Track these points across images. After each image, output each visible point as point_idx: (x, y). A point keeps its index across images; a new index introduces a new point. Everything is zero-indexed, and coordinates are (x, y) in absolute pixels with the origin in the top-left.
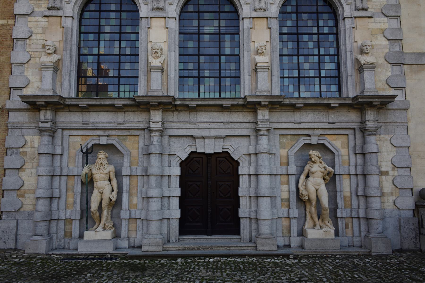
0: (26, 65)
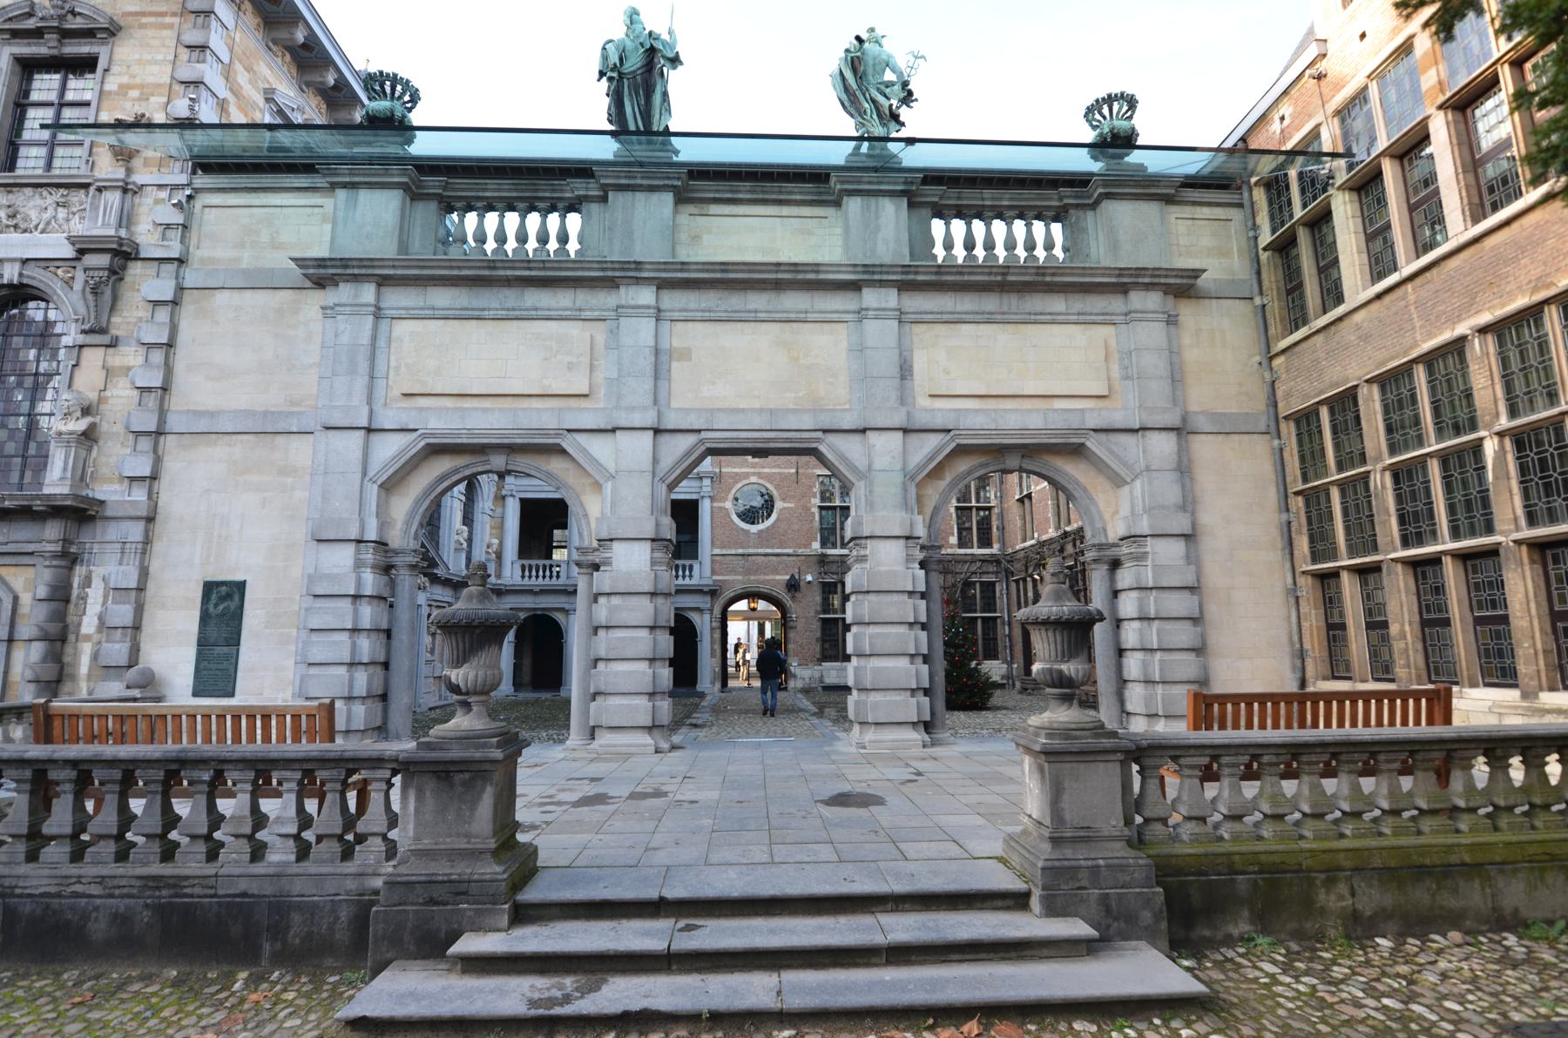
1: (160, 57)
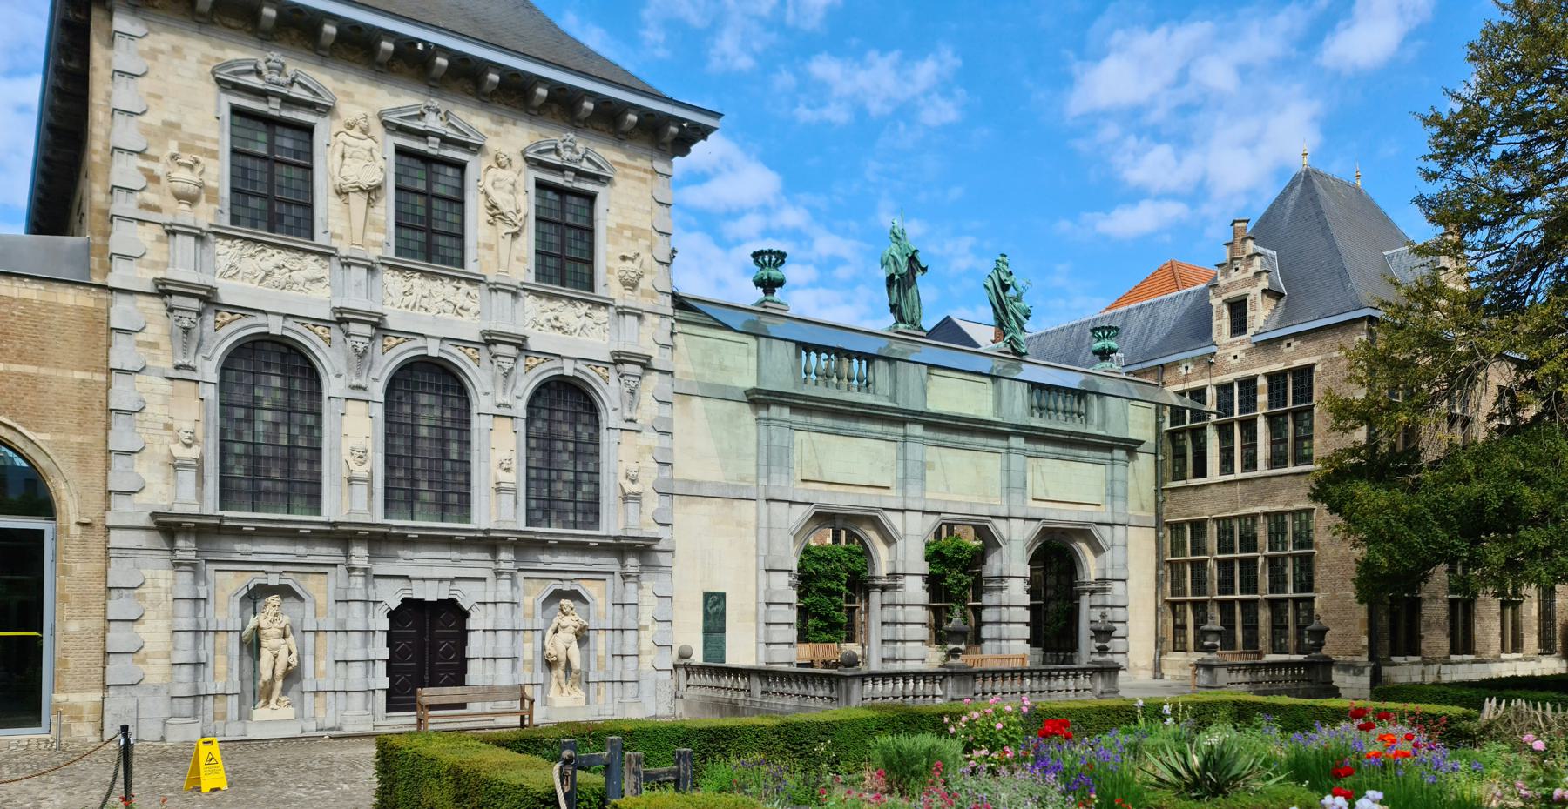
0: (136, 455)
1: (641, 207)
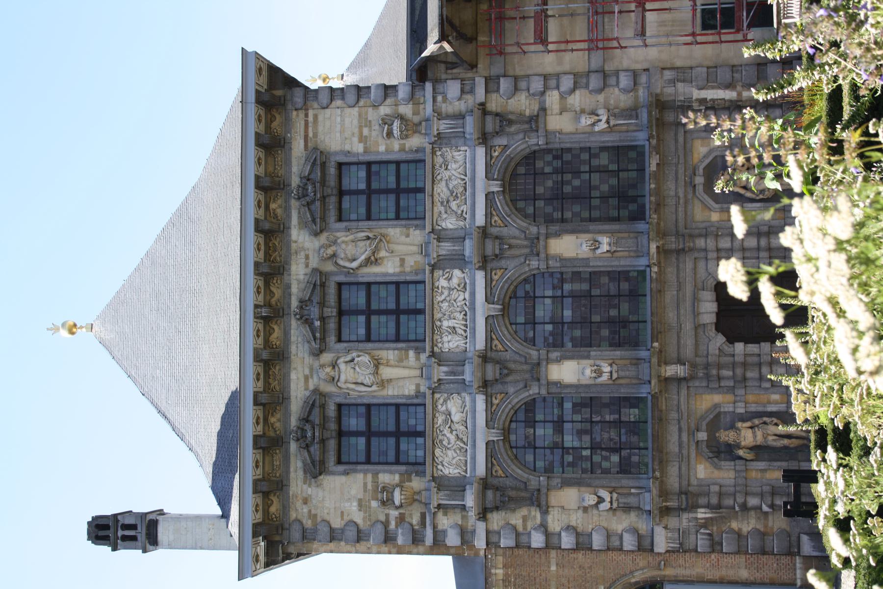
1: (339, 119)
